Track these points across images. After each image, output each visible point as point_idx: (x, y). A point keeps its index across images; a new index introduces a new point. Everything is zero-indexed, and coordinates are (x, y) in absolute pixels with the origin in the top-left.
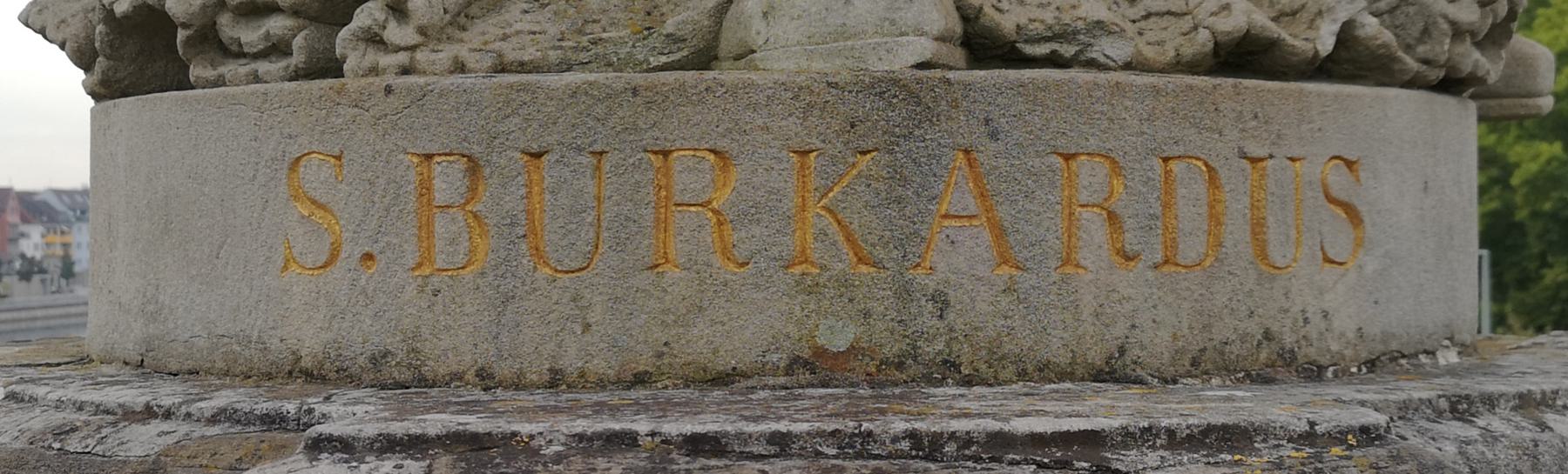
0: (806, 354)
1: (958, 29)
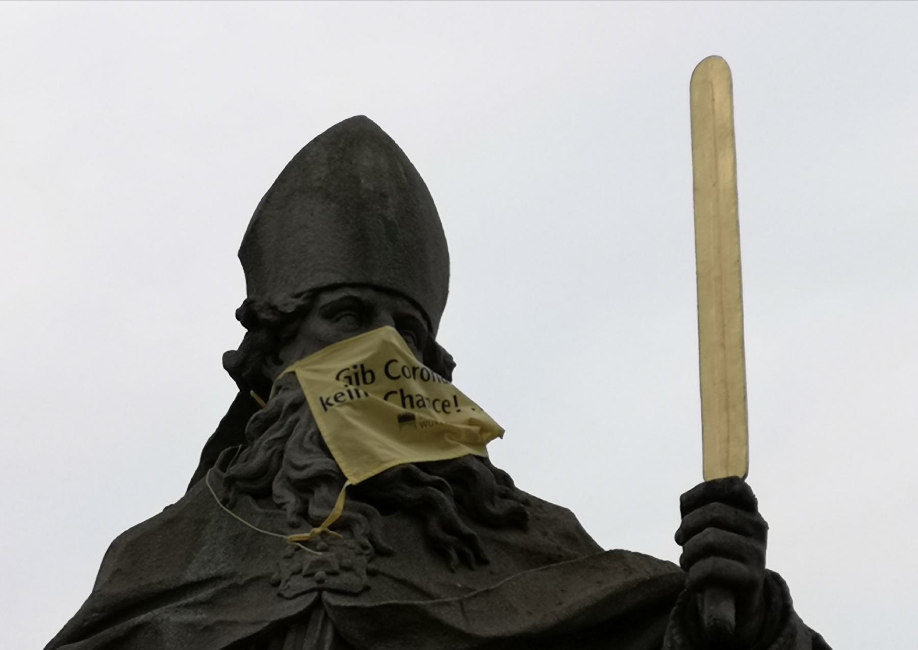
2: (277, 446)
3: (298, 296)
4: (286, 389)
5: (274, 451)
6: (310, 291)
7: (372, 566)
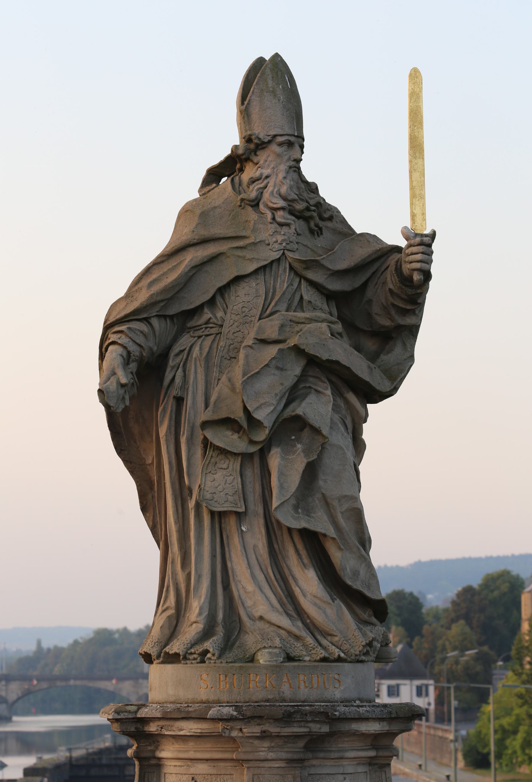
0: (267, 699)
1: (286, 656)
2: (261, 190)
3: (269, 136)
4: (262, 168)
5: (259, 192)
6: (274, 135)
7: (297, 241)
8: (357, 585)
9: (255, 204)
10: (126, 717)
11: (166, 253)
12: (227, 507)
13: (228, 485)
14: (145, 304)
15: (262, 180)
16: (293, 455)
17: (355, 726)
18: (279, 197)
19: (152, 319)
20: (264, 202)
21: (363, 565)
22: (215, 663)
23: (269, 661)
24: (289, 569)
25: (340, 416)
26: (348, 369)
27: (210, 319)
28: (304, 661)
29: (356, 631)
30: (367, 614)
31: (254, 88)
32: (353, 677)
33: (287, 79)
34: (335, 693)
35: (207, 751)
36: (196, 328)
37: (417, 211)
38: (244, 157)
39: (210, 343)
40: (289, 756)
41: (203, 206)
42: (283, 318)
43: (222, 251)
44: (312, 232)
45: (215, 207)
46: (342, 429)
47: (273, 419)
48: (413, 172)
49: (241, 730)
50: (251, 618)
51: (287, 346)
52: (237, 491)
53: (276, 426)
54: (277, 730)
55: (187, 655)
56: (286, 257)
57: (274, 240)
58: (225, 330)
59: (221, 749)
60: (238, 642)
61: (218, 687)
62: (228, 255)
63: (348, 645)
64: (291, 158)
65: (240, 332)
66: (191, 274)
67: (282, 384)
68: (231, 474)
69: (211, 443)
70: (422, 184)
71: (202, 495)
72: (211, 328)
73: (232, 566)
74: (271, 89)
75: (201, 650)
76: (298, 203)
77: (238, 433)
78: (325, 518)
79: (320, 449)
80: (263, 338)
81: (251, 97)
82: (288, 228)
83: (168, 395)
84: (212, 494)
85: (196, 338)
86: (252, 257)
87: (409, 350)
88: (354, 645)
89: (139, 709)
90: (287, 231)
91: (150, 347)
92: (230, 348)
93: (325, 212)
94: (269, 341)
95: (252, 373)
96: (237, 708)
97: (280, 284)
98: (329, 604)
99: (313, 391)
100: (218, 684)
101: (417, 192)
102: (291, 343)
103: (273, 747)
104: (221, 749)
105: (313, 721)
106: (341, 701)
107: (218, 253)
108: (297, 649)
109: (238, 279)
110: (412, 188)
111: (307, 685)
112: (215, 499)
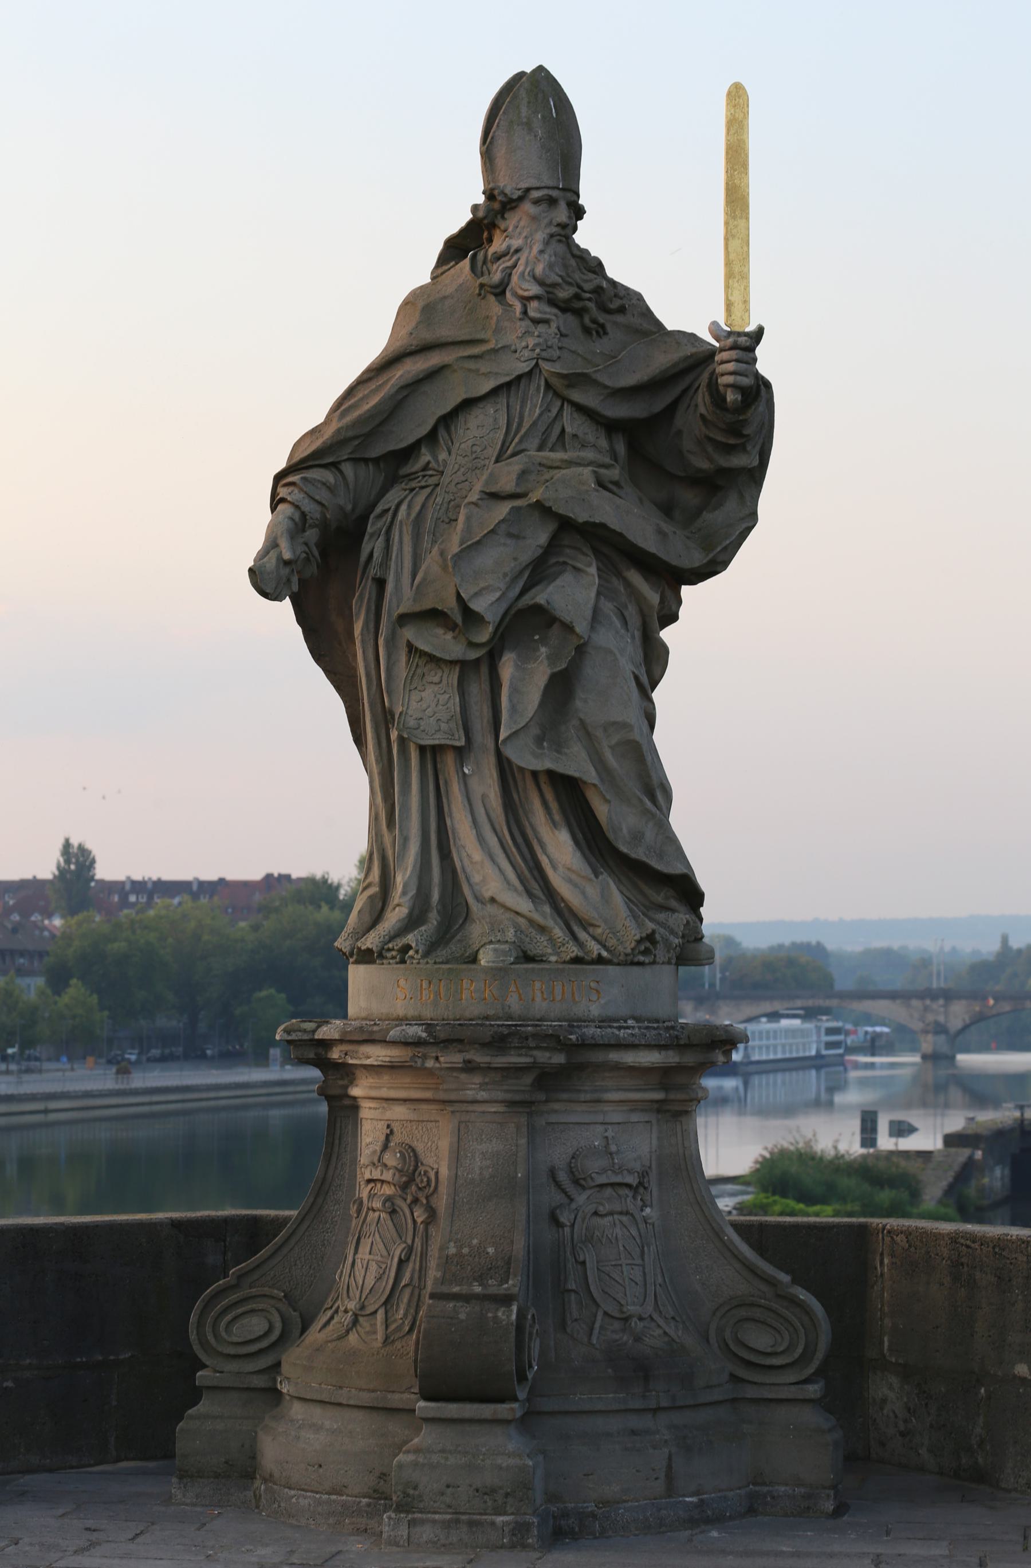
1: (521, 954)
2: (508, 271)
3: (519, 189)
4: (511, 238)
7: (560, 345)
8: (639, 854)
9: (500, 291)
10: (300, 1038)
11: (375, 366)
12: (439, 739)
13: (441, 707)
14: (329, 442)
15: (510, 255)
16: (534, 663)
17: (614, 1056)
18: (532, 280)
19: (343, 464)
20: (512, 288)
21: (650, 824)
22: (418, 963)
23: (493, 962)
24: (534, 830)
25: (615, 604)
26: (621, 535)
27: (429, 463)
28: (550, 962)
29: (628, 919)
30: (662, 894)
31: (500, 119)
32: (623, 986)
33: (552, 103)
34: (591, 1008)
35: (403, 1088)
36: (410, 477)
37: (736, 297)
38: (486, 222)
39: (424, 498)
40: (508, 1096)
41: (429, 296)
42: (527, 461)
43: (446, 363)
44: (587, 331)
45: (445, 298)
46: (618, 623)
47: (501, 611)
48: (730, 239)
49: (437, 1058)
50: (478, 899)
51: (527, 503)
52: (453, 716)
53: (507, 620)
54: (487, 1059)
55: (384, 952)
56: (540, 371)
57: (524, 344)
58: (445, 479)
59: (422, 1086)
60: (460, 934)
61: (419, 998)
62: (456, 367)
63: (615, 940)
64: (553, 221)
65: (467, 483)
66: (400, 397)
67: (515, 559)
68: (445, 692)
69: (416, 647)
70: (744, 256)
71: (402, 722)
72: (431, 476)
73: (452, 824)
74: (525, 120)
75: (400, 945)
76: (562, 288)
77: (453, 632)
78: (584, 754)
79: (573, 654)
80: (493, 490)
81: (494, 132)
82: (547, 326)
83: (366, 575)
84: (417, 721)
85: (407, 492)
86: (489, 370)
87: (749, 504)
88: (624, 940)
89: (318, 1027)
90: (544, 330)
91: (340, 505)
92: (450, 506)
93: (611, 301)
94: (503, 494)
95: (469, 543)
96: (429, 1027)
97: (530, 410)
98: (590, 880)
99: (569, 568)
100: (419, 993)
101: (736, 269)
102: (534, 497)
103: (487, 1084)
104: (422, 1086)
105: (537, 1048)
106: (600, 1019)
107: (441, 365)
108: (540, 945)
109: (468, 404)
110: (728, 263)
111: (545, 996)
112: (422, 728)
